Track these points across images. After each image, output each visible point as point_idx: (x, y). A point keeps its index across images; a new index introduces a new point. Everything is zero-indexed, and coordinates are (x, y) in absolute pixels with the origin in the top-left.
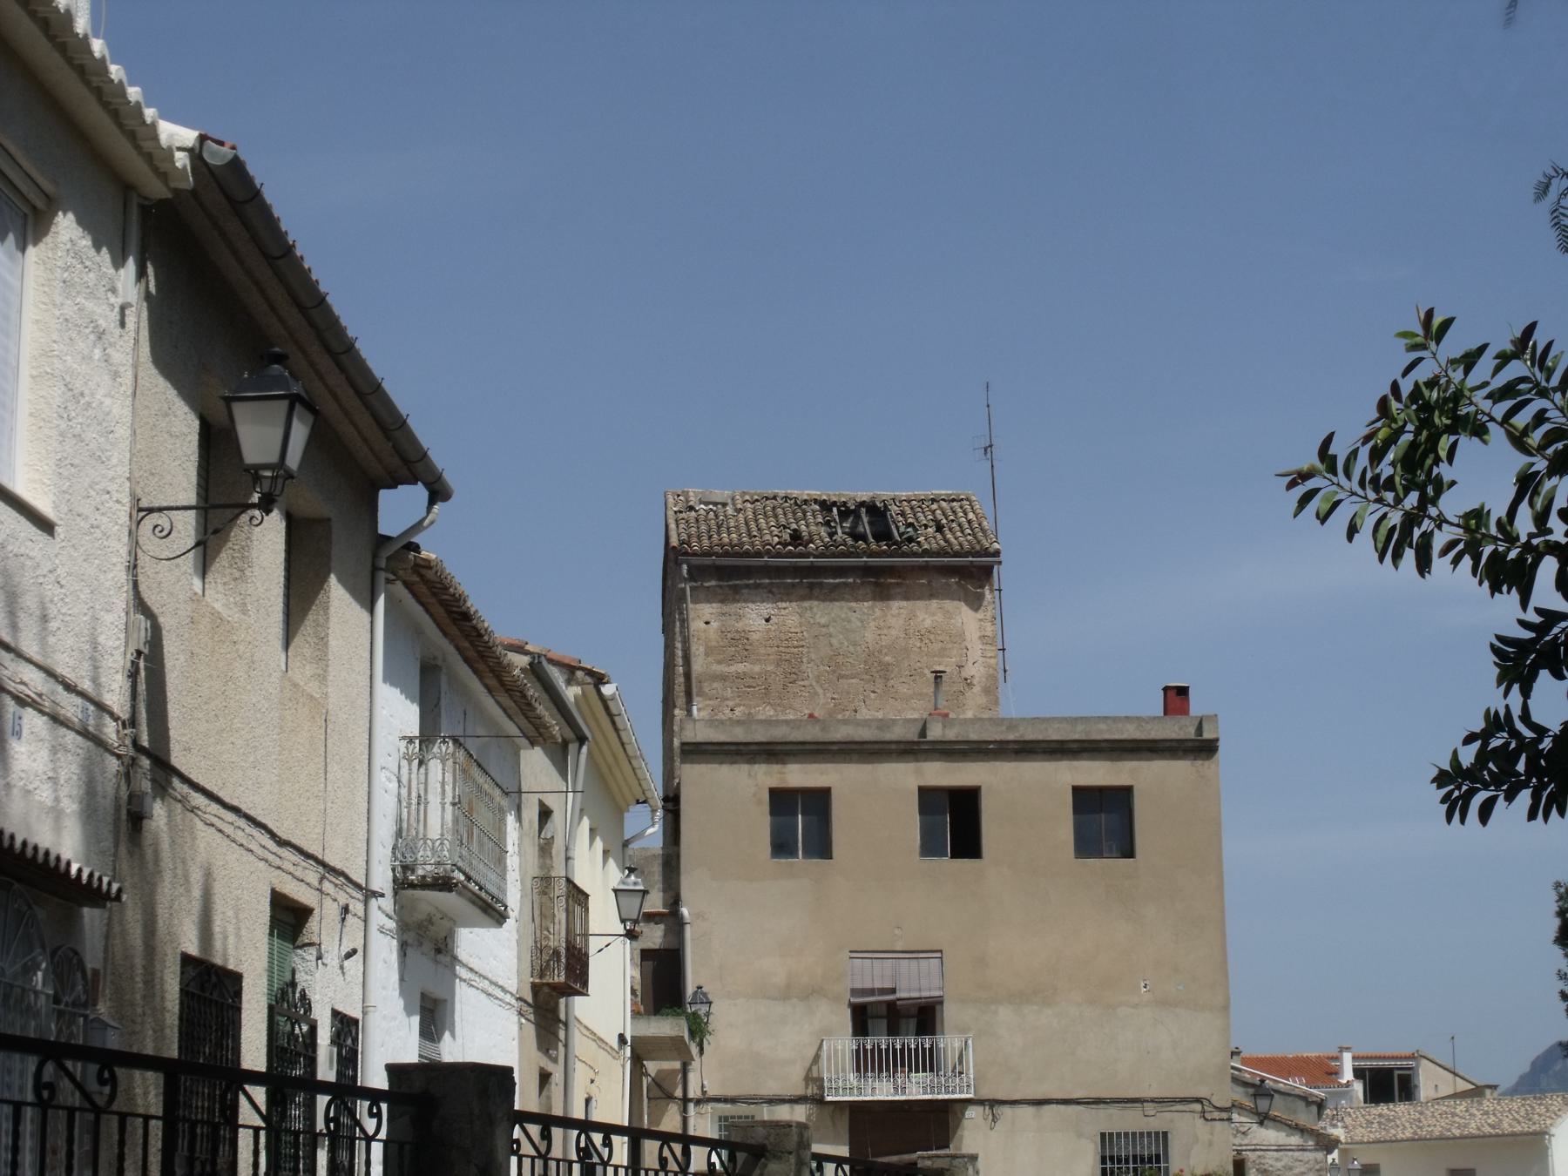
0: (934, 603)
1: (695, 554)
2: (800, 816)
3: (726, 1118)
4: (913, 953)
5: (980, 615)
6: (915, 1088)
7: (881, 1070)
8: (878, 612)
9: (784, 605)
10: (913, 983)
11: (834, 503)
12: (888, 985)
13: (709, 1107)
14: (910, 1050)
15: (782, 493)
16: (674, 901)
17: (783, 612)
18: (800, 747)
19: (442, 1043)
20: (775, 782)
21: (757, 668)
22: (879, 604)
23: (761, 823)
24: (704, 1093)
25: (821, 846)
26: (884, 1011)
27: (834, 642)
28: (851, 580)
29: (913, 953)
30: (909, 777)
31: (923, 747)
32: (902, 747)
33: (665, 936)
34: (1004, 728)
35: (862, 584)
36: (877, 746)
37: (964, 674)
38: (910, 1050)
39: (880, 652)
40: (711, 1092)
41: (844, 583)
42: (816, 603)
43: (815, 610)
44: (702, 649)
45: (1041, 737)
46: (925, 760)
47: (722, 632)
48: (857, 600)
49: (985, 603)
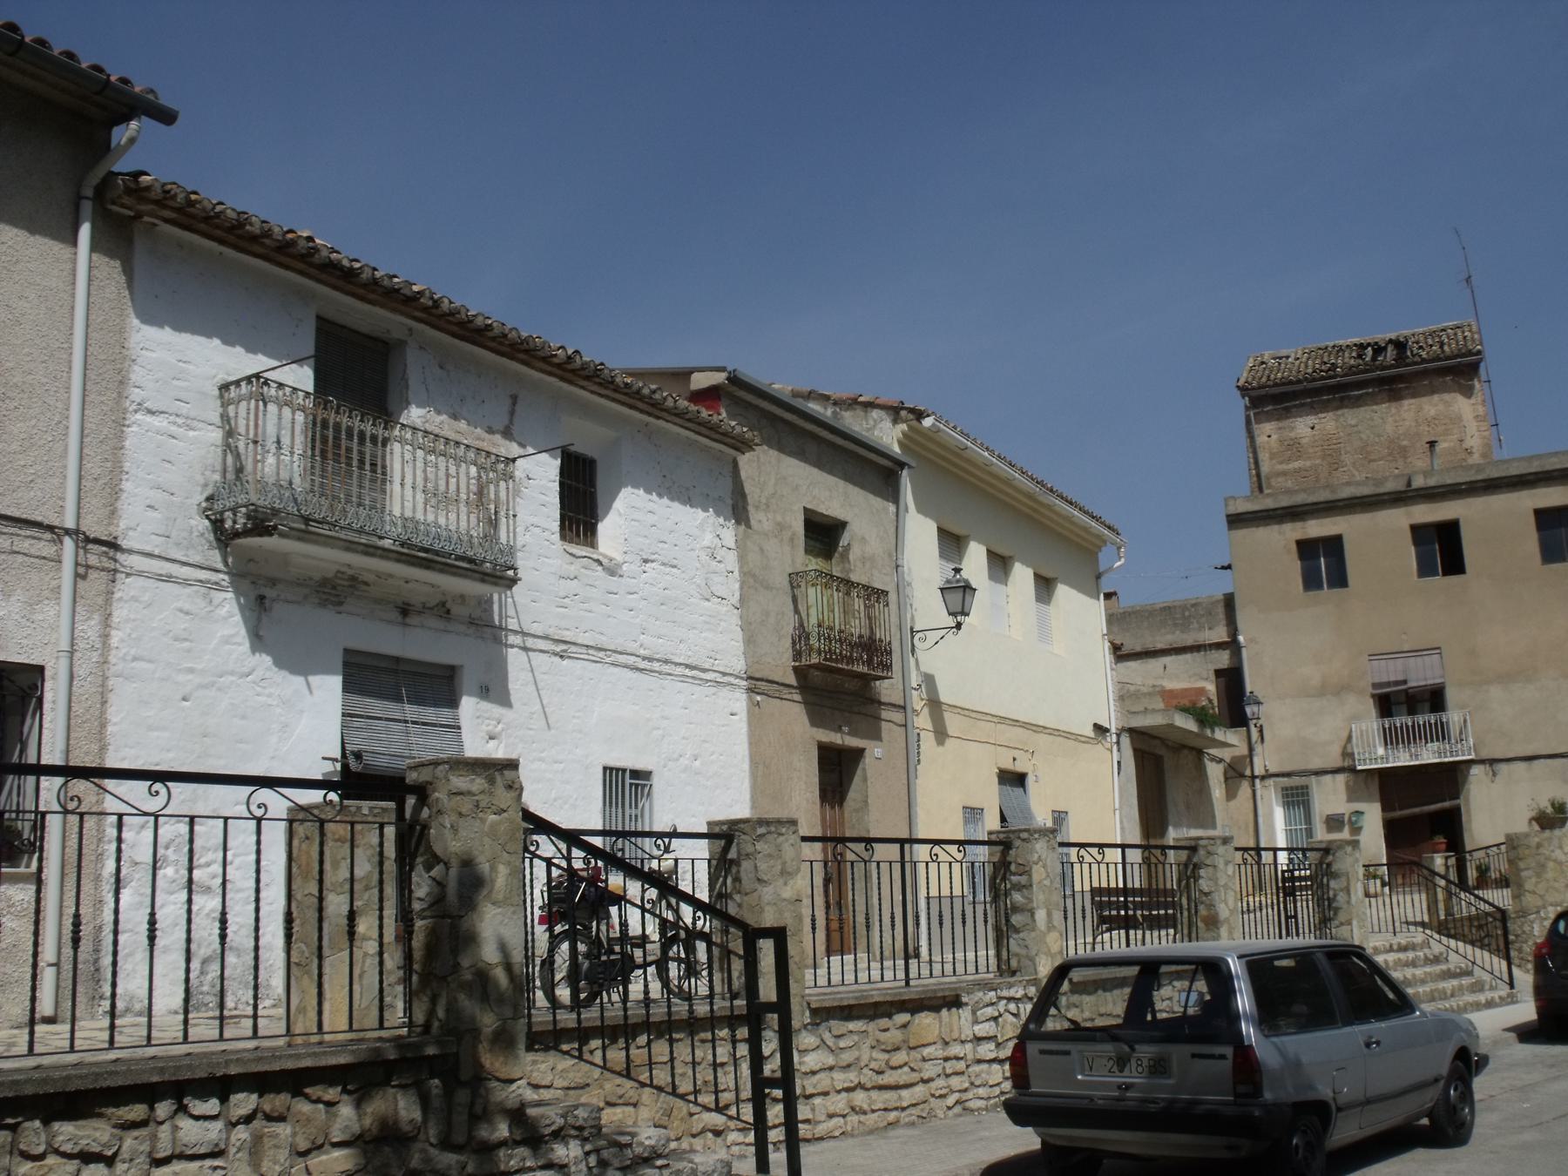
0: (1436, 397)
1: (1253, 389)
2: (1322, 559)
3: (1287, 789)
4: (1417, 652)
5: (1473, 401)
6: (1429, 755)
7: (1397, 743)
8: (1393, 410)
9: (1323, 415)
10: (1420, 674)
11: (1369, 345)
12: (1400, 678)
13: (1271, 782)
14: (1419, 726)
15: (1331, 344)
16: (1233, 631)
17: (1323, 420)
18: (1315, 507)
19: (460, 708)
20: (1299, 535)
21: (1308, 463)
22: (1394, 404)
23: (1293, 567)
24: (1267, 771)
25: (1339, 578)
26: (1403, 698)
27: (1363, 436)
28: (1370, 390)
29: (1417, 652)
30: (1400, 519)
31: (1410, 494)
32: (1393, 496)
33: (1231, 658)
34: (1473, 472)
35: (1380, 391)
36: (1373, 499)
37: (1464, 446)
38: (1419, 726)
39: (1398, 438)
40: (1272, 770)
41: (1367, 393)
42: (1346, 410)
43: (1346, 415)
44: (1267, 455)
45: (1504, 474)
46: (1412, 504)
47: (1281, 441)
48: (1377, 404)
49: (1476, 391)
